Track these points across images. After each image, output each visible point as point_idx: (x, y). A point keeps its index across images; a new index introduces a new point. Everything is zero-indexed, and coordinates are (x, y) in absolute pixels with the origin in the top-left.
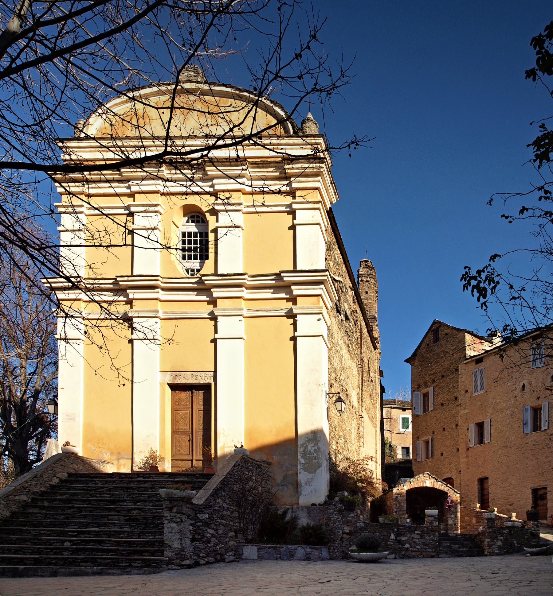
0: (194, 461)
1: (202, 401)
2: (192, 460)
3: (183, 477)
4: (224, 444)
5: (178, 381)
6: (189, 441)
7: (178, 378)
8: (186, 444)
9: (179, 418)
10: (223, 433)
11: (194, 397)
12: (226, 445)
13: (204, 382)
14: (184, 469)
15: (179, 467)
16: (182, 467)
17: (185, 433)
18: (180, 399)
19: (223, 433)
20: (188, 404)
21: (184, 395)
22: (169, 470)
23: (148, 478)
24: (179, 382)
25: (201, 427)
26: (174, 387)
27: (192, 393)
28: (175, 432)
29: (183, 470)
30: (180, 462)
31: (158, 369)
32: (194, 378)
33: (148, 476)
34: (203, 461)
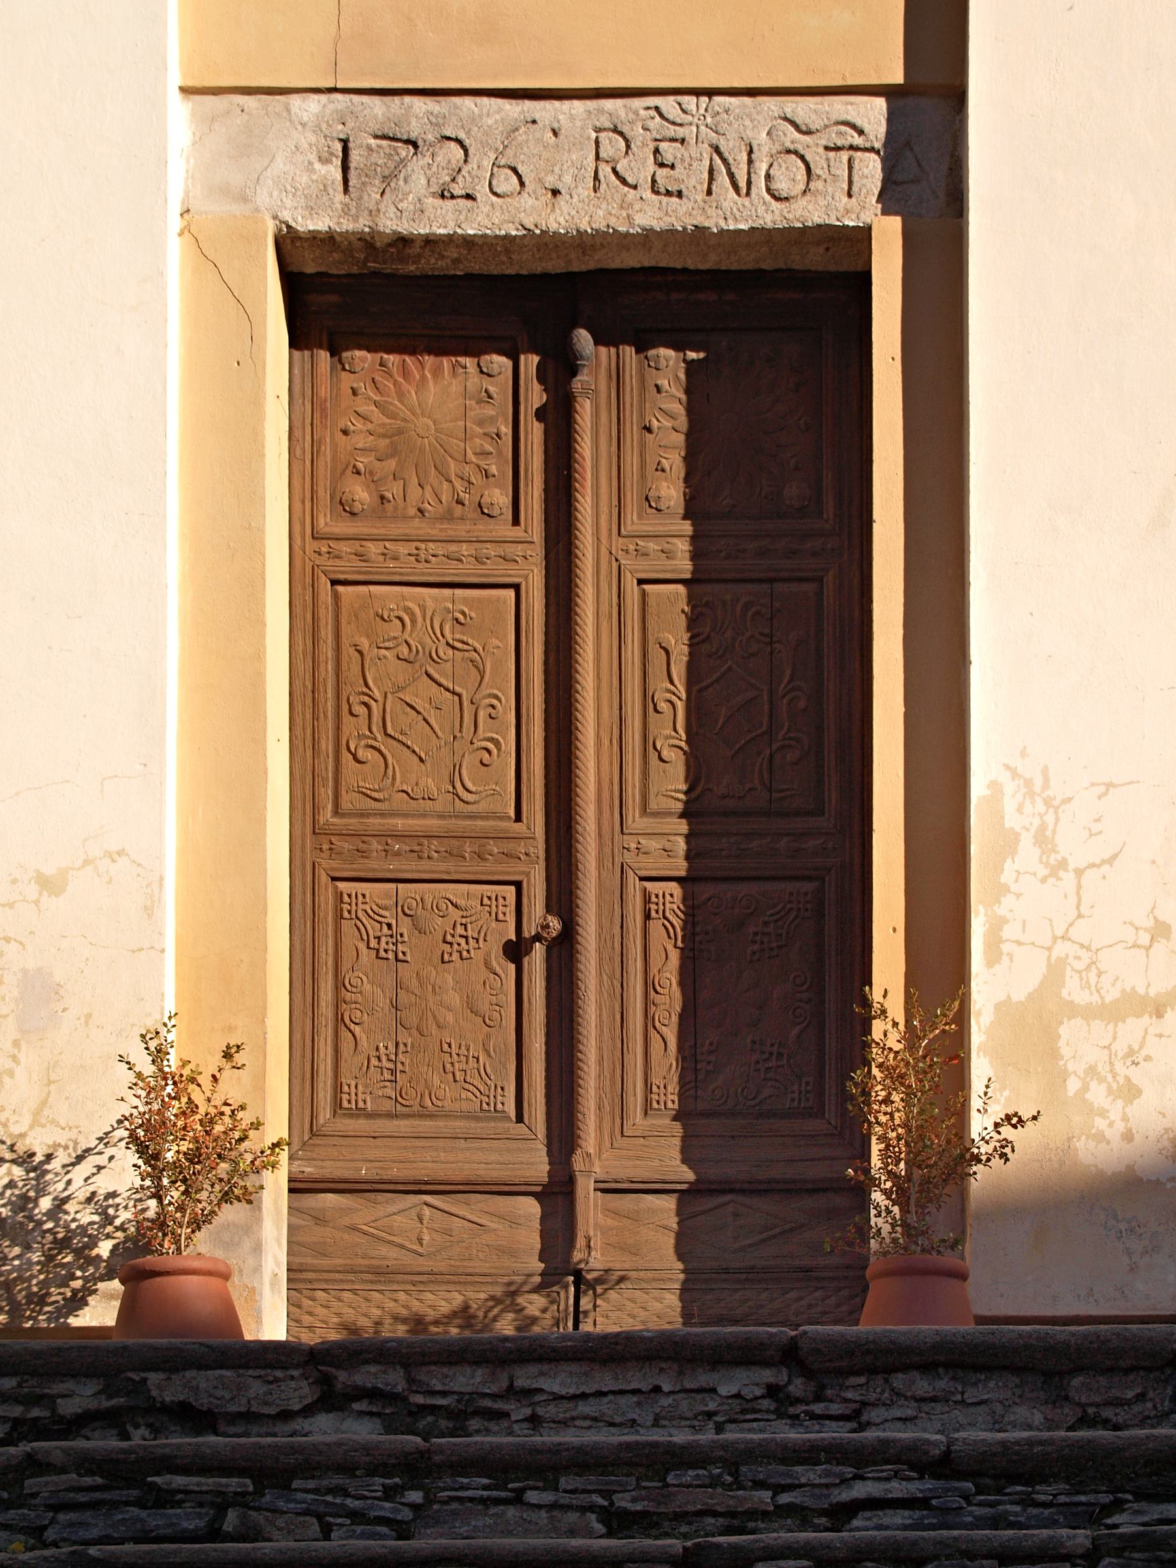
0: (591, 1208)
1: (675, 462)
2: (558, 1194)
3: (992, 1389)
4: (1055, 972)
5: (415, 209)
6: (516, 951)
7: (419, 178)
8: (477, 1001)
9: (385, 671)
10: (1044, 840)
11: (585, 412)
12: (1074, 991)
13: (768, 215)
14: (439, 1302)
15: (382, 1274)
16: (433, 1278)
17: (457, 852)
18: (396, 443)
19: (1044, 840)
20: (500, 498)
21: (460, 399)
22: (270, 1322)
23: (461, 1415)
24: (443, 220)
25: (672, 781)
26: (346, 298)
27: (561, 370)
28: (338, 848)
29: (418, 1323)
30: (399, 1213)
31: (175, 79)
32: (641, 168)
33: (467, 1380)
34: (687, 1196)
